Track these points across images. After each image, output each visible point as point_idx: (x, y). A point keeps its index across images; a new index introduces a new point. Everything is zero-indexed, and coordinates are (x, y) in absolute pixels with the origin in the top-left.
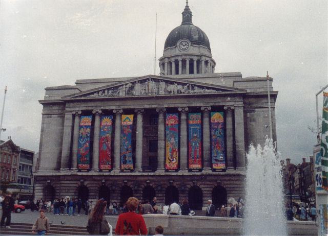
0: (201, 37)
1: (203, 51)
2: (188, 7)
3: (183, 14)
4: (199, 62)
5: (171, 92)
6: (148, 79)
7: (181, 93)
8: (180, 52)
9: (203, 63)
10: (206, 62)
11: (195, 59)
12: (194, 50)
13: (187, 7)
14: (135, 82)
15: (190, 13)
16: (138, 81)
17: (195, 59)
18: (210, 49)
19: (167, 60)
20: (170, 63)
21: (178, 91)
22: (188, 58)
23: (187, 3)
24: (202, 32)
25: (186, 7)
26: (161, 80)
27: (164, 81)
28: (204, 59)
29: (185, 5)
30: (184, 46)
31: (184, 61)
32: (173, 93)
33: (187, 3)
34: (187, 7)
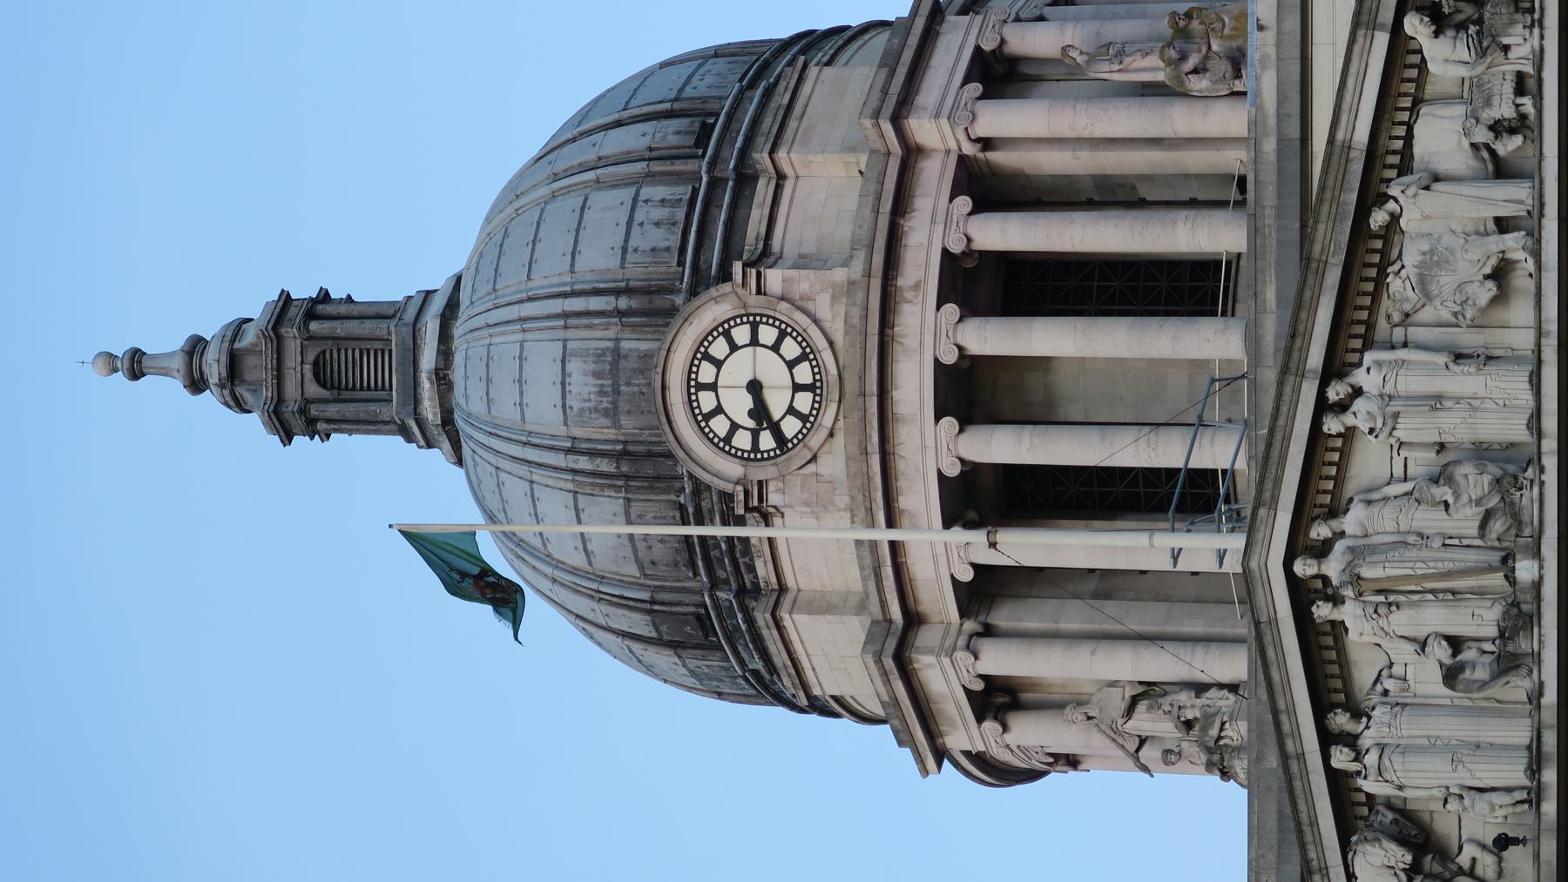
0: (652, 155)
2: (196, 346)
5: (1501, 273)
6: (1302, 594)
7: (1519, 125)
8: (840, 439)
9: (999, 118)
14: (1339, 782)
16: (1328, 739)
18: (809, 43)
21: (1501, 170)
23: (136, 365)
24: (581, 129)
25: (196, 384)
26: (1322, 407)
27: (1334, 369)
29: (166, 389)
30: (755, 387)
32: (1513, 243)
33: (136, 365)
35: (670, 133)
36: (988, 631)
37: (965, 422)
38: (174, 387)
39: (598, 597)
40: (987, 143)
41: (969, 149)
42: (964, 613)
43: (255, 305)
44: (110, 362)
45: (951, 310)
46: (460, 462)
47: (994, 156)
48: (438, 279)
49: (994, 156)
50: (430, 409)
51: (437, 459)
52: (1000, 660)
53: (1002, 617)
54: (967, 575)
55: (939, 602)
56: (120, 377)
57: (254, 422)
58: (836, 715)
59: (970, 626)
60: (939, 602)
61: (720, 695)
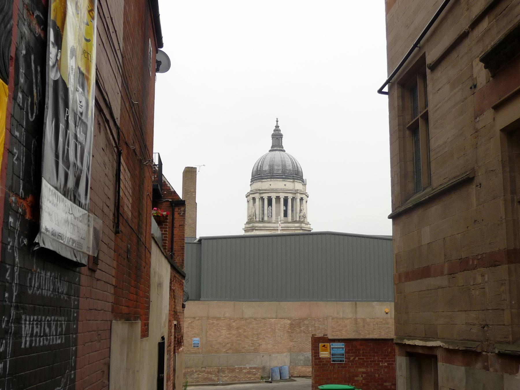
1: (298, 186)
2: (279, 127)
3: (273, 136)
4: (293, 199)
9: (298, 200)
10: (302, 199)
11: (290, 196)
12: (289, 185)
13: (277, 127)
15: (281, 136)
17: (290, 196)
19: (257, 196)
20: (262, 199)
22: (282, 196)
23: (277, 121)
25: (276, 127)
28: (299, 196)
31: (278, 198)
33: (277, 121)
34: (277, 127)
35: (296, 172)
36: (259, 199)
37: (275, 198)
38: (275, 125)
39: (261, 166)
40: (296, 199)
41: (296, 198)
42: (261, 197)
43: (282, 132)
44: (277, 119)
45: (284, 197)
46: (270, 151)
47: (295, 199)
48: (284, 149)
49: (295, 199)
50: (275, 148)
51: (270, 149)
52: (257, 200)
53: (260, 200)
54: (264, 198)
55: (262, 195)
56: (276, 120)
57: (273, 132)
58: (251, 182)
59: (260, 197)
60: (262, 195)
61: (252, 173)
